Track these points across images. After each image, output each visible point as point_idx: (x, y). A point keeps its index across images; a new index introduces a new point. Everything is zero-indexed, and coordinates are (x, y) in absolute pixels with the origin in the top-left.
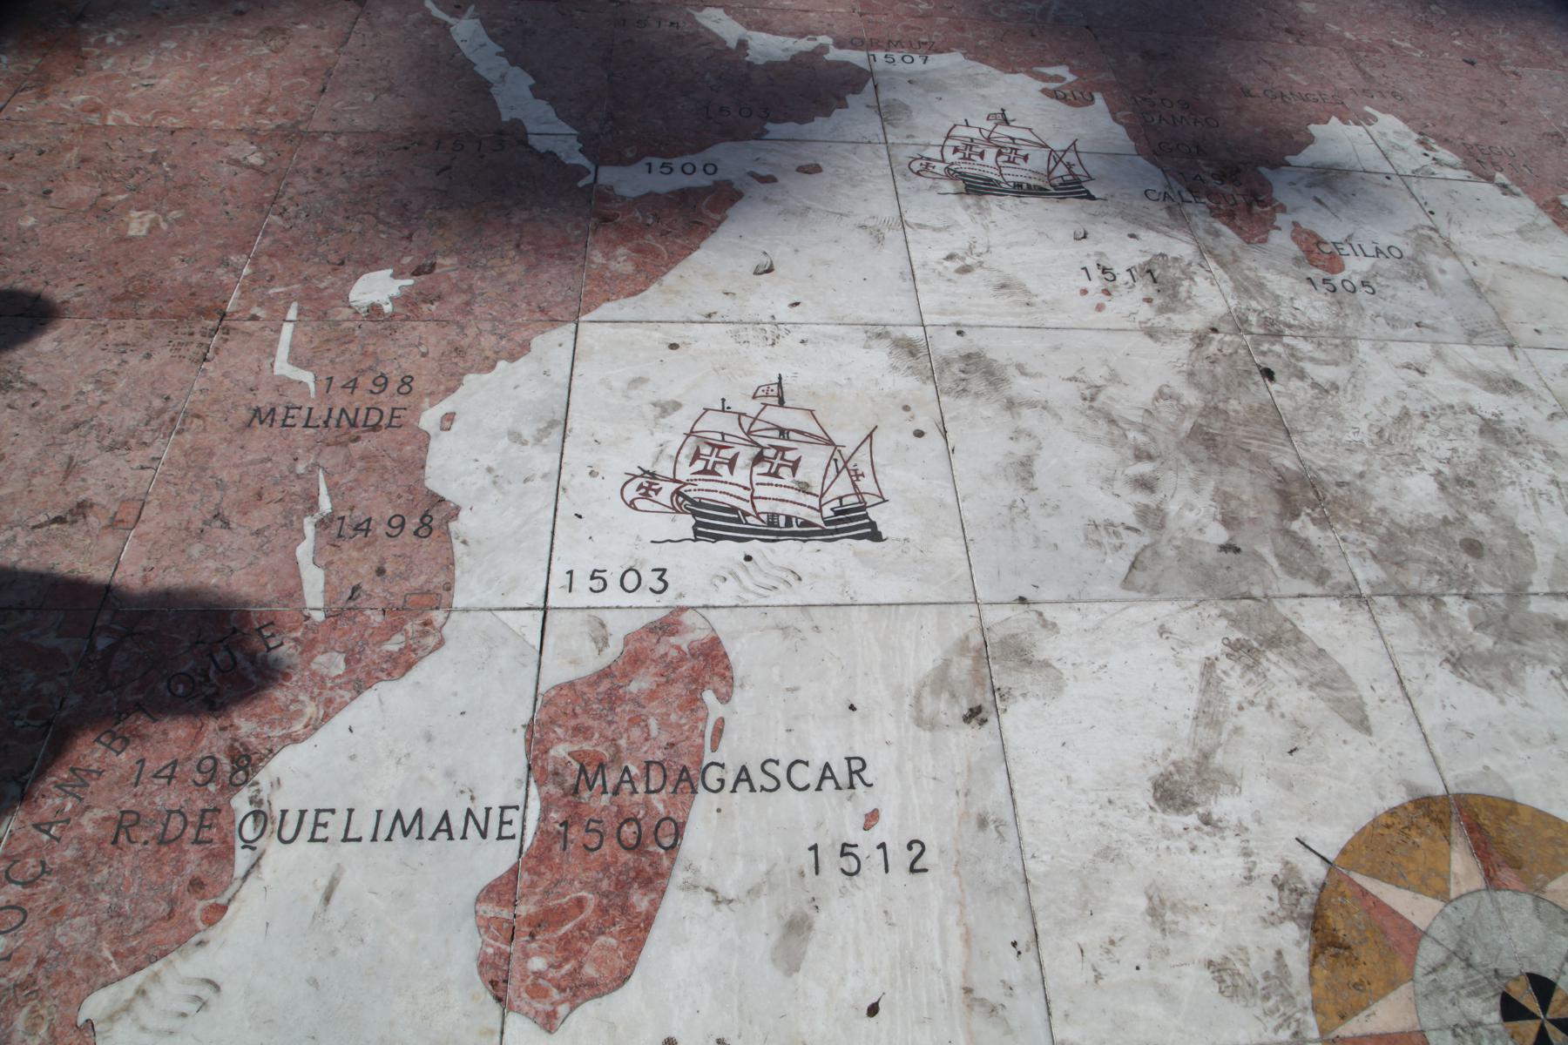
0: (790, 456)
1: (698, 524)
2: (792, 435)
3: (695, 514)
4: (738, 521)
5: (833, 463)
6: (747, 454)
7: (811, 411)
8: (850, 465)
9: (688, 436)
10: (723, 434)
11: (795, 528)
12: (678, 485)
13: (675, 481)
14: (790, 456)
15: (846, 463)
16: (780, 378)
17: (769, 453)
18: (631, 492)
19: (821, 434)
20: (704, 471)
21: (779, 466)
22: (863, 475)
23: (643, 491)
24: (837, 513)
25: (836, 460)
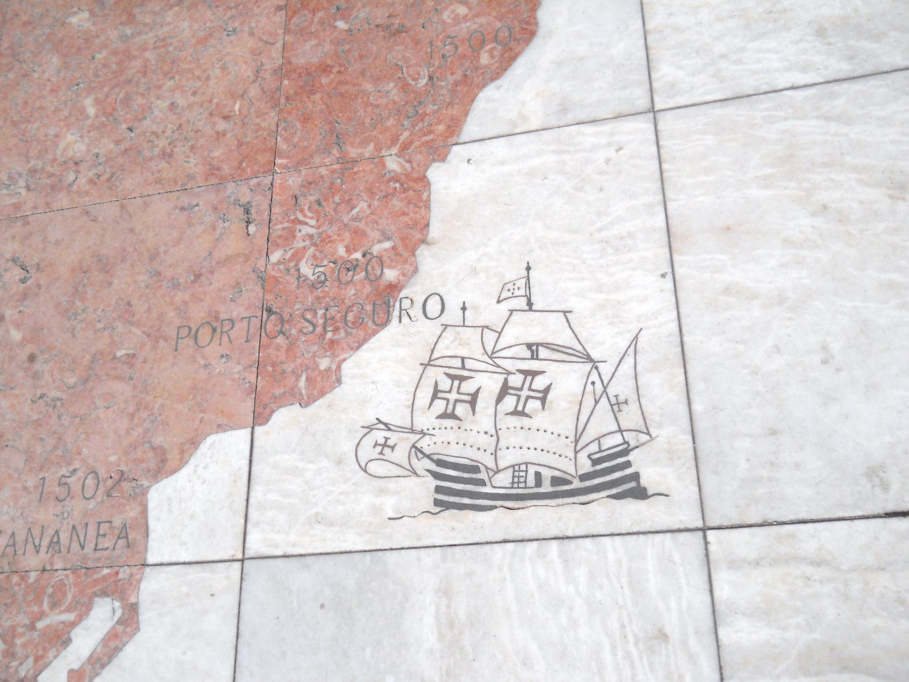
0: (540, 383)
1: (438, 490)
2: (543, 353)
3: (436, 476)
4: (482, 483)
5: (589, 387)
6: (490, 384)
7: (565, 312)
8: (611, 391)
9: (425, 365)
10: (463, 359)
11: (546, 488)
12: (414, 438)
13: (412, 431)
14: (540, 383)
15: (605, 388)
16: (528, 269)
17: (516, 380)
18: (368, 451)
19: (579, 348)
20: (443, 416)
21: (528, 398)
22: (626, 402)
23: (379, 449)
24: (595, 462)
25: (593, 383)
